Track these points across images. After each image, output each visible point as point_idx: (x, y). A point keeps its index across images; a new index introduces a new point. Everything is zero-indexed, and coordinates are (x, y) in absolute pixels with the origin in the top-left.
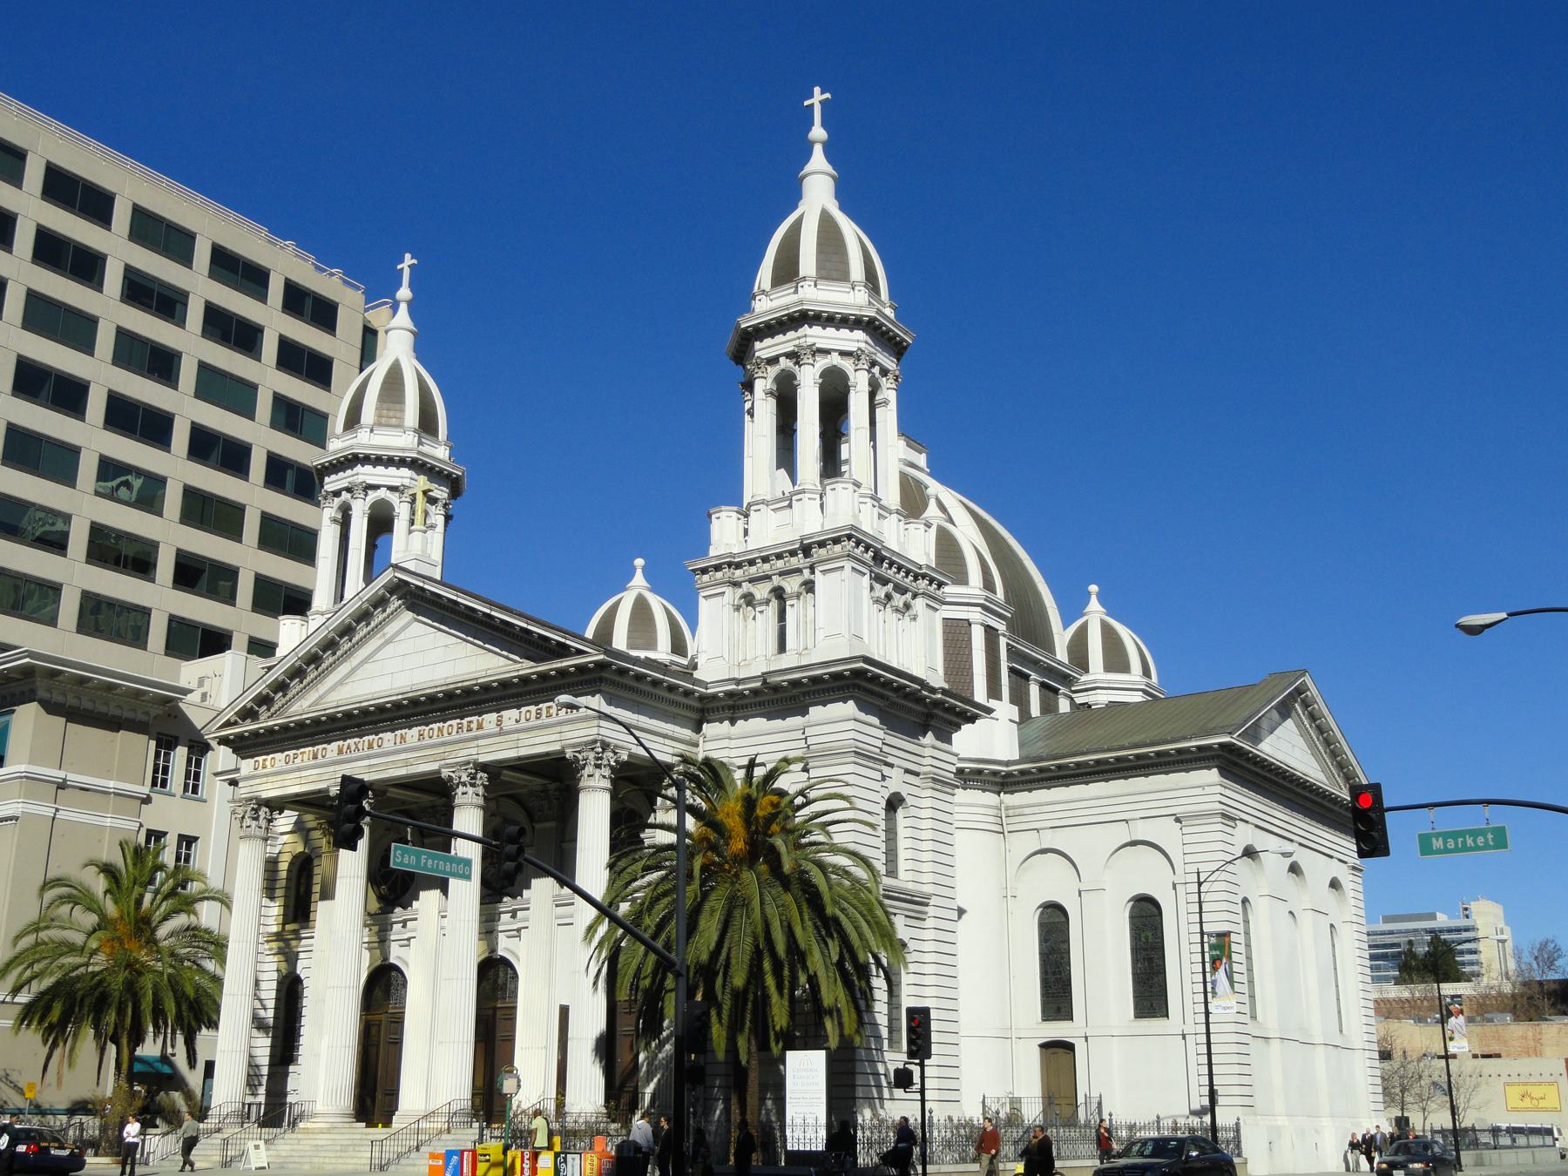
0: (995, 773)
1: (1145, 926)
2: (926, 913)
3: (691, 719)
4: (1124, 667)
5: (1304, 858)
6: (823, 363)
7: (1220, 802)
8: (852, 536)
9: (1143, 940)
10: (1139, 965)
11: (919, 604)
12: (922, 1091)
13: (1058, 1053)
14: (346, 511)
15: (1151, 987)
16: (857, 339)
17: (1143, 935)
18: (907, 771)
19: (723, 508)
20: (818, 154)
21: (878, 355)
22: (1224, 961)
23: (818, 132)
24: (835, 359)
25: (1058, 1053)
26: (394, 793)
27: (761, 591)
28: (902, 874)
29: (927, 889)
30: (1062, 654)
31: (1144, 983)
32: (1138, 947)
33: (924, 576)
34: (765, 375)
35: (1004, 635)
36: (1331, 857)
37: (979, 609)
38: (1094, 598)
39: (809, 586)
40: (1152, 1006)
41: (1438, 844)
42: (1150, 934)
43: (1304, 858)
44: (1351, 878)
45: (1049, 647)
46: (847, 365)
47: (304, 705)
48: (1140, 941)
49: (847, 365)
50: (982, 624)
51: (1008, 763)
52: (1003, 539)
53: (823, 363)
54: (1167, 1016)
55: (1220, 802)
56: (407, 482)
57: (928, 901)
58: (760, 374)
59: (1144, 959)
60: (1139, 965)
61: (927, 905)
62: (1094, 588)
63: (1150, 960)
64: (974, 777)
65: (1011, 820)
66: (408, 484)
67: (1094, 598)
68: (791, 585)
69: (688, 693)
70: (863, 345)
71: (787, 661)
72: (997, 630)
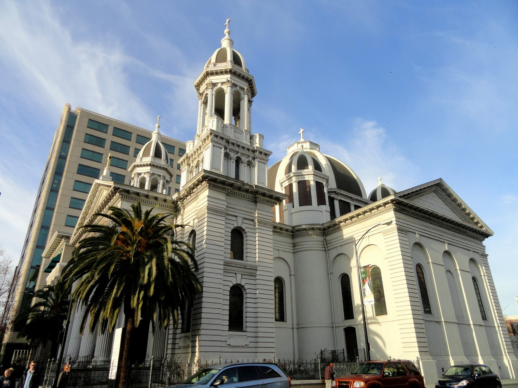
10: (376, 294)
15: (381, 302)
17: (376, 282)
18: (244, 218)
19: (188, 142)
22: (367, 279)
31: (378, 301)
32: (375, 287)
36: (470, 250)
40: (382, 310)
42: (378, 281)
43: (452, 249)
44: (482, 258)
48: (375, 284)
54: (387, 314)
59: (377, 292)
60: (376, 294)
63: (379, 292)
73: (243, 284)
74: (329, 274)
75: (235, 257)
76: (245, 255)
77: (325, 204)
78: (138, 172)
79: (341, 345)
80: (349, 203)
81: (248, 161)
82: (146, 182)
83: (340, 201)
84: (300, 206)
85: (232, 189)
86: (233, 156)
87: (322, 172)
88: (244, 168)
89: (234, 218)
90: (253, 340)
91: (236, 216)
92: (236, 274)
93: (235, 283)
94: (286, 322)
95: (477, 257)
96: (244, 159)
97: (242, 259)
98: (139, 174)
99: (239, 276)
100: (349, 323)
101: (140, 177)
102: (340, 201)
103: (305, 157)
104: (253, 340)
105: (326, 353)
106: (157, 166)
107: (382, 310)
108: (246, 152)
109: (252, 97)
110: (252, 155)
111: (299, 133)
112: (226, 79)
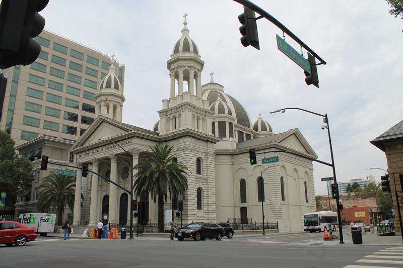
4: (266, 130)
5: (297, 167)
6: (184, 69)
8: (186, 104)
12: (181, 217)
13: (244, 210)
14: (101, 105)
24: (186, 68)
25: (244, 210)
26: (104, 161)
27: (171, 117)
30: (252, 128)
39: (180, 114)
41: (265, 161)
45: (249, 127)
46: (189, 69)
47: (86, 145)
49: (189, 69)
53: (184, 69)
64: (218, 154)
68: (177, 115)
69: (156, 138)
71: (176, 130)
75: (197, 173)
76: (201, 172)
79: (238, 216)
80: (242, 132)
83: (239, 131)
86: (196, 116)
88: (201, 122)
89: (198, 153)
90: (206, 214)
91: (199, 151)
95: (308, 171)
96: (201, 117)
97: (200, 174)
100: (244, 205)
102: (239, 131)
104: (206, 214)
106: (117, 96)
108: (202, 113)
110: (204, 113)
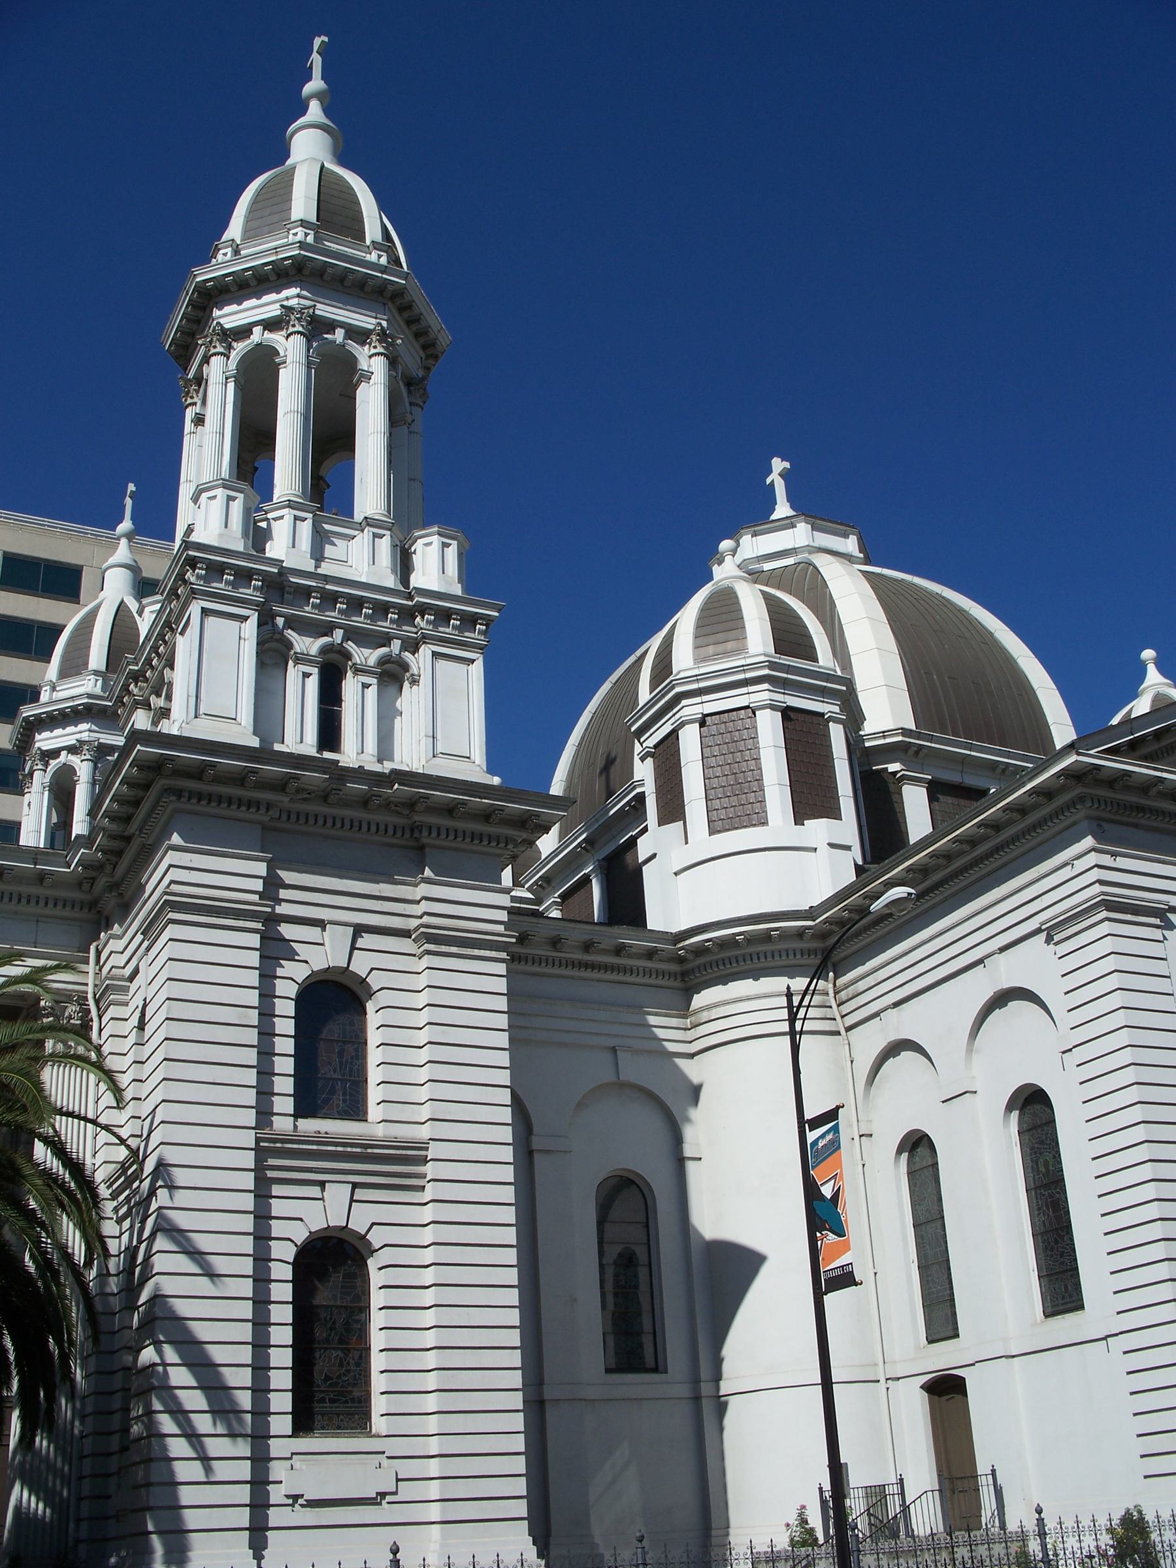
0: (800, 933)
1: (1042, 1142)
2: (424, 1176)
3: (74, 919)
7: (1101, 882)
9: (1042, 1169)
11: (421, 661)
16: (291, 295)
20: (315, 112)
21: (319, 306)
23: (315, 84)
24: (257, 335)
28: (374, 1112)
29: (424, 1133)
31: (1052, 1249)
32: (1037, 1185)
33: (423, 610)
34: (195, 400)
35: (837, 721)
37: (766, 686)
38: (1152, 670)
40: (1066, 1287)
50: (773, 707)
51: (811, 913)
52: (961, 611)
55: (1101, 882)
56: (85, 736)
57: (423, 1153)
58: (189, 401)
61: (424, 1161)
62: (1148, 654)
65: (846, 1008)
66: (87, 739)
67: (1152, 670)
70: (293, 302)
72: (823, 715)
73: (359, 1224)
74: (857, 1138)
77: (833, 812)
78: (44, 748)
81: (383, 661)
82: (77, 786)
84: (712, 831)
85: (292, 800)
87: (816, 660)
91: (320, 924)
92: (322, 1184)
93: (317, 1224)
94: (666, 1372)
98: (48, 755)
99: (338, 1193)
100: (944, 1357)
101: (54, 764)
103: (737, 597)
105: (857, 1500)
107: (1066, 1287)
109: (431, 362)
111: (768, 481)
112: (277, 306)
